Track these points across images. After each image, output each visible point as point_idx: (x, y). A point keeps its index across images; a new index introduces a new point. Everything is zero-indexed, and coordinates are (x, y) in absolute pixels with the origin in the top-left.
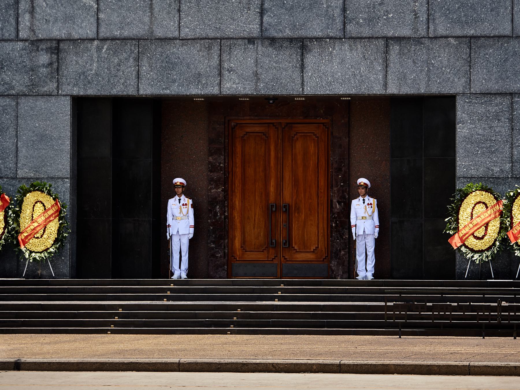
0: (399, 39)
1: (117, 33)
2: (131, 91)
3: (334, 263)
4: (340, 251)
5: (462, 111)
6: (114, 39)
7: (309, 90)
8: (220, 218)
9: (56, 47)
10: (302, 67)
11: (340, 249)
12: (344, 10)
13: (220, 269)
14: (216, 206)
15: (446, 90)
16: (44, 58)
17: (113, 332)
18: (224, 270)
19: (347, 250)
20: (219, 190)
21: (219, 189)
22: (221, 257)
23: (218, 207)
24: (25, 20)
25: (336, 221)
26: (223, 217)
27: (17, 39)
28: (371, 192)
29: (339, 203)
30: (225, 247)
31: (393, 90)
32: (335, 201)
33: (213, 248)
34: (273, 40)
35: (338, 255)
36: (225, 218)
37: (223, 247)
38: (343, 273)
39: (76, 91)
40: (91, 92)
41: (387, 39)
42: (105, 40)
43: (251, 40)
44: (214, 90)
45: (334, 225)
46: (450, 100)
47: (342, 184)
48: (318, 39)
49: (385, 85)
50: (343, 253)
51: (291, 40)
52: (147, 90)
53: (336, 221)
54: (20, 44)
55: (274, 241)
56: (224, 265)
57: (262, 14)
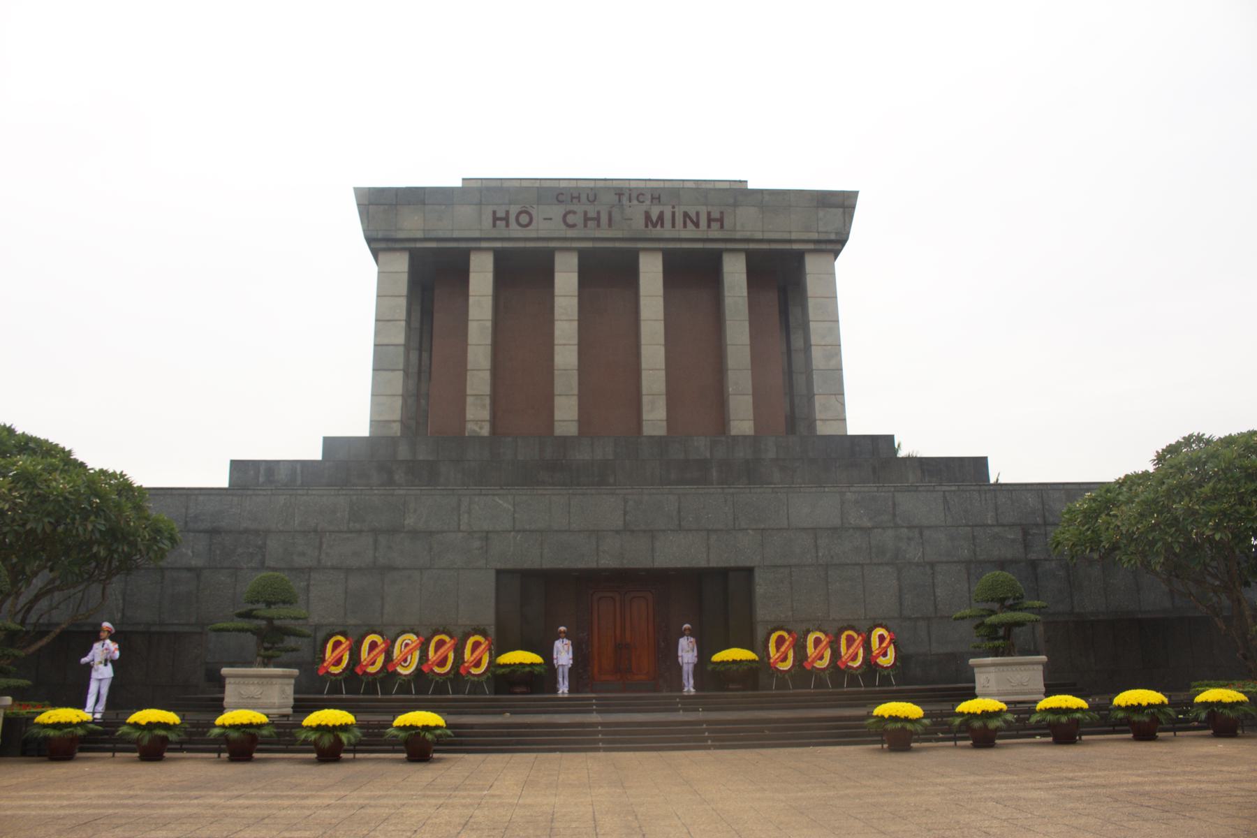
0: (716, 531)
1: (527, 527)
2: (536, 566)
5: (759, 577)
6: (524, 531)
7: (657, 565)
9: (486, 536)
10: (653, 550)
12: (679, 512)
15: (748, 564)
16: (477, 544)
17: (606, 750)
24: (465, 518)
27: (459, 531)
28: (692, 633)
31: (713, 564)
34: (633, 531)
39: (499, 566)
40: (509, 566)
41: (708, 531)
42: (519, 531)
43: (617, 532)
44: (593, 565)
46: (750, 571)
48: (664, 531)
49: (708, 561)
51: (645, 531)
52: (547, 565)
54: (460, 535)
57: (625, 514)
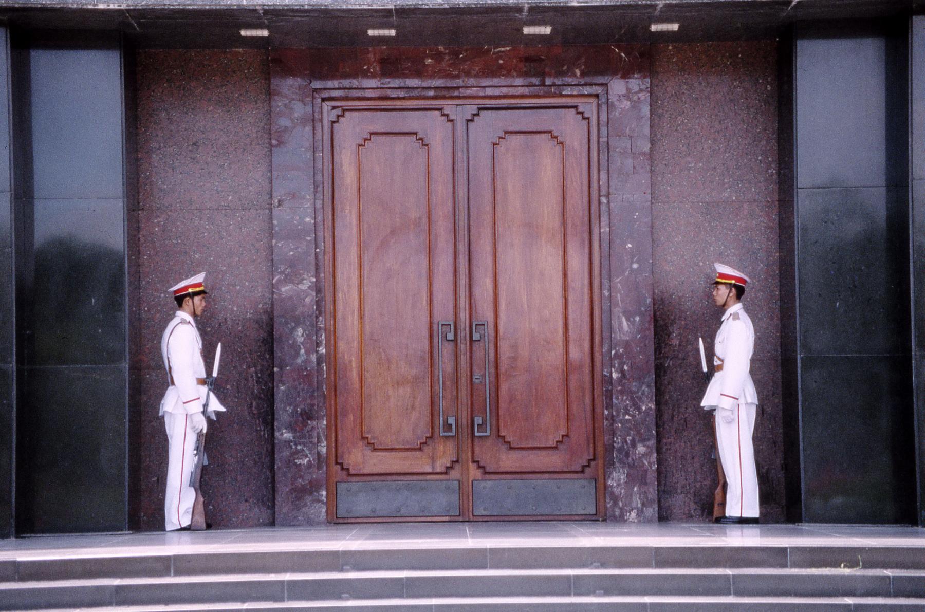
3: (617, 478)
4: (634, 445)
8: (307, 361)
11: (633, 441)
13: (308, 499)
14: (294, 329)
18: (319, 501)
19: (652, 442)
20: (304, 287)
21: (301, 282)
22: (310, 465)
23: (300, 331)
25: (622, 364)
26: (314, 357)
29: (629, 315)
30: (319, 441)
32: (617, 311)
33: (288, 442)
35: (627, 455)
36: (319, 363)
37: (315, 440)
38: (643, 504)
45: (615, 375)
47: (635, 266)
50: (641, 449)
53: (622, 364)
55: (451, 421)
56: (318, 489)
